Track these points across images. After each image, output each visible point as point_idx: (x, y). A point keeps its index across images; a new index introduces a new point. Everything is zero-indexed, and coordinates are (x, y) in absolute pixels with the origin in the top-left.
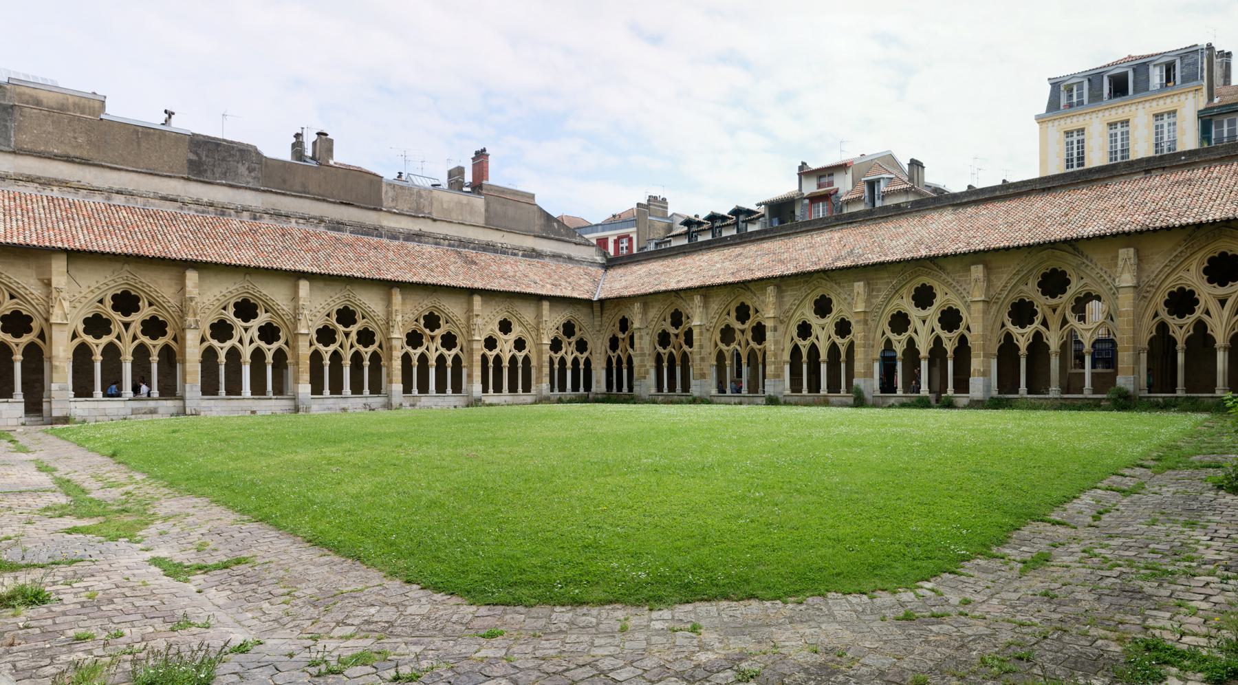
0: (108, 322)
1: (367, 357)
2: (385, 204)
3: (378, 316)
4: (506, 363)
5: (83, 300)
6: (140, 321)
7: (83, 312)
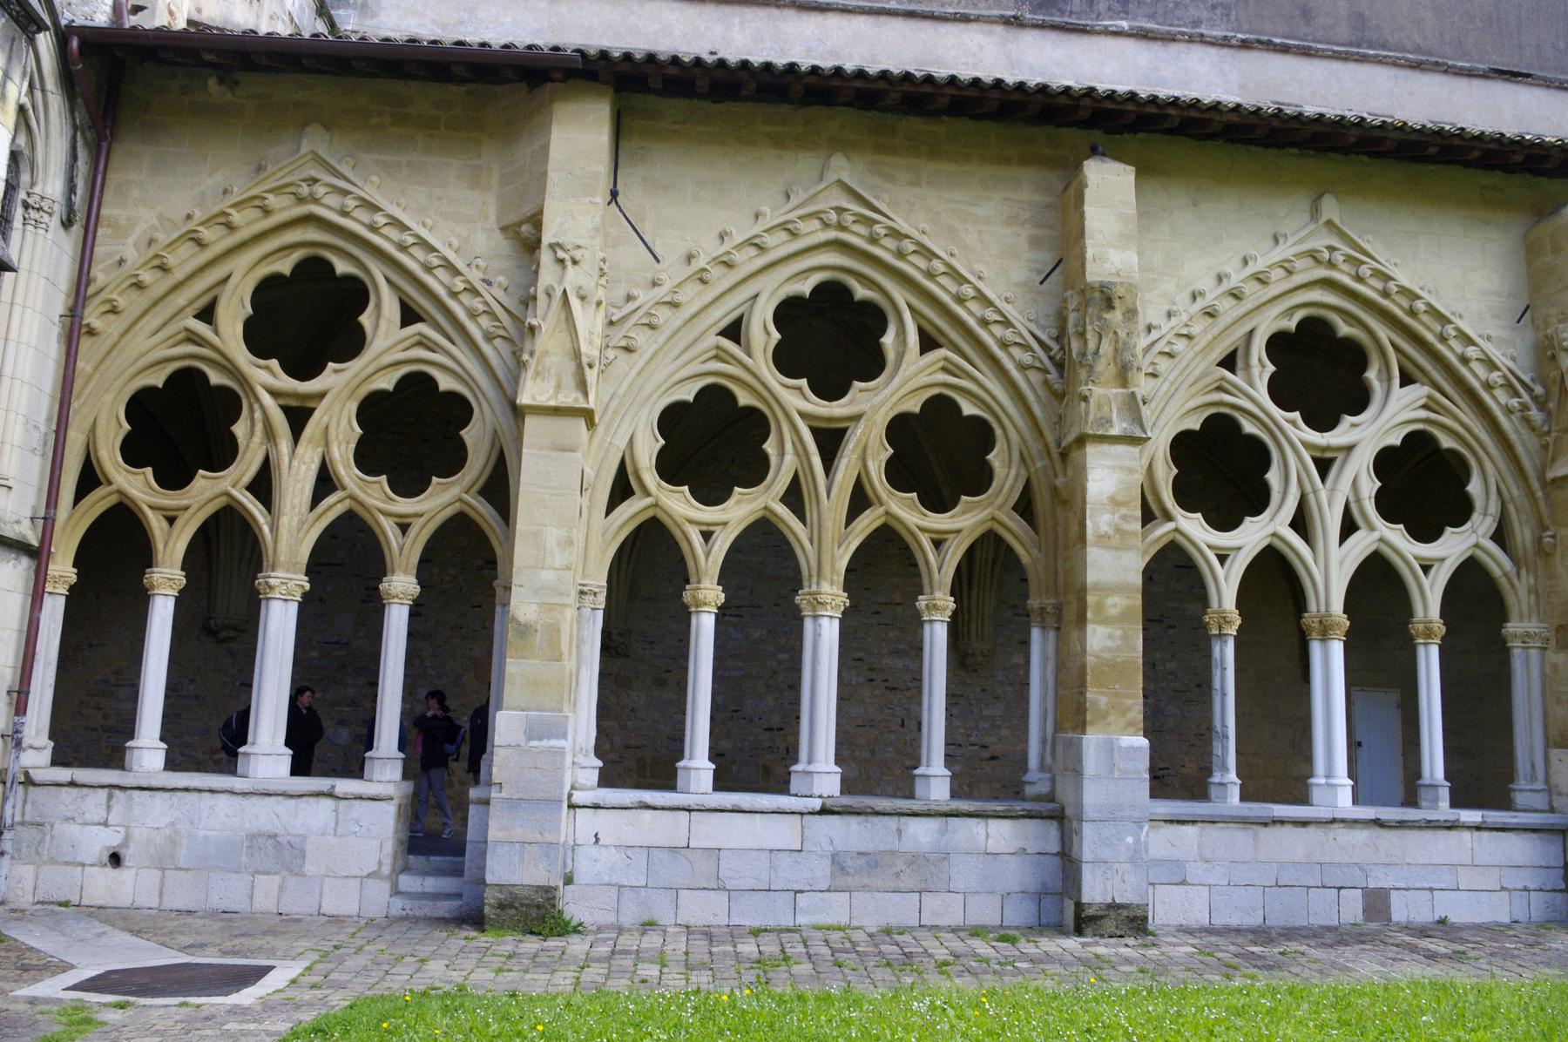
0: (755, 424)
5: (663, 314)
6: (882, 419)
7: (660, 374)
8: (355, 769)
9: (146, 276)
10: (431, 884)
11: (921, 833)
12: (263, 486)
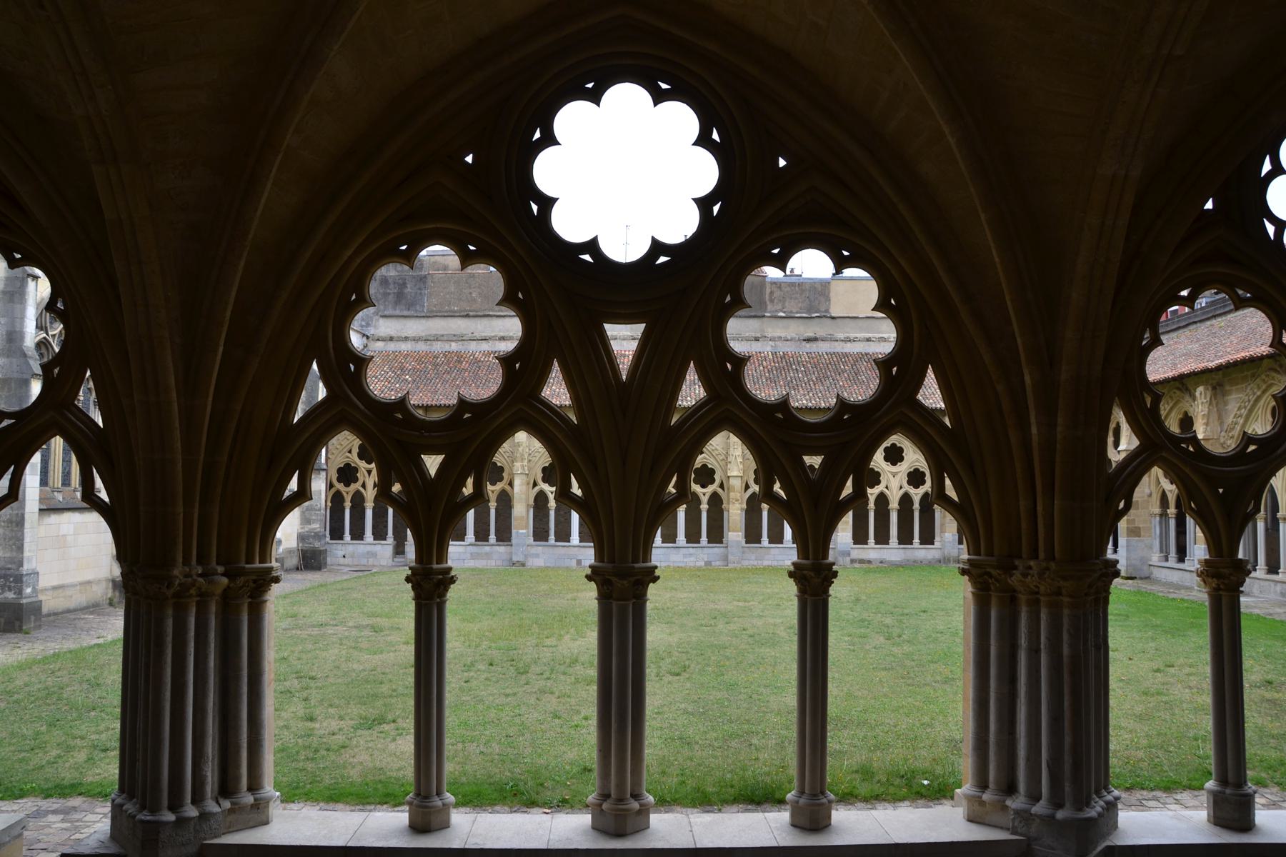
1: (705, 500)
2: (769, 307)
3: (716, 449)
4: (894, 505)
8: (385, 539)
9: (338, 447)
10: (400, 560)
11: (487, 548)
12: (364, 486)
